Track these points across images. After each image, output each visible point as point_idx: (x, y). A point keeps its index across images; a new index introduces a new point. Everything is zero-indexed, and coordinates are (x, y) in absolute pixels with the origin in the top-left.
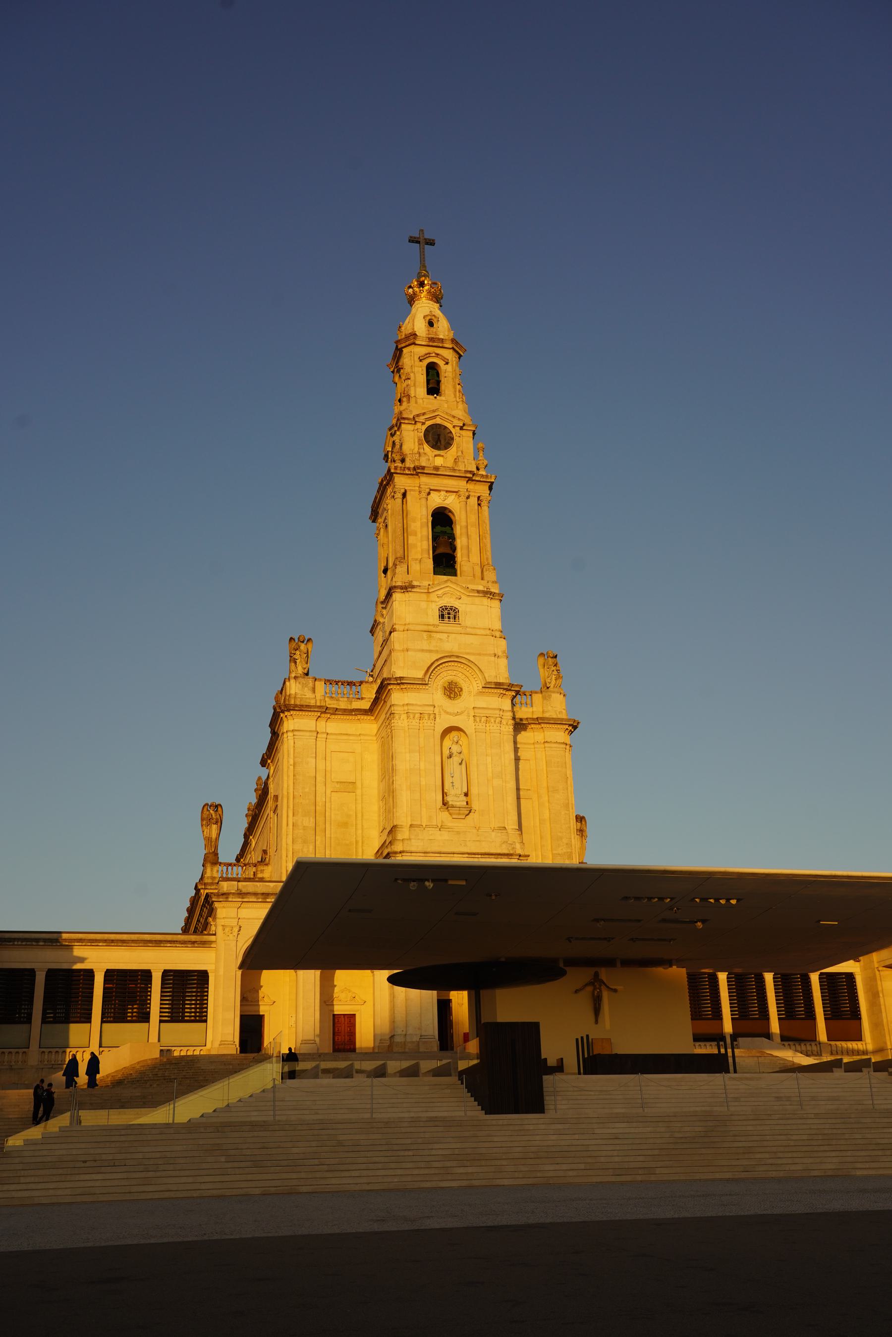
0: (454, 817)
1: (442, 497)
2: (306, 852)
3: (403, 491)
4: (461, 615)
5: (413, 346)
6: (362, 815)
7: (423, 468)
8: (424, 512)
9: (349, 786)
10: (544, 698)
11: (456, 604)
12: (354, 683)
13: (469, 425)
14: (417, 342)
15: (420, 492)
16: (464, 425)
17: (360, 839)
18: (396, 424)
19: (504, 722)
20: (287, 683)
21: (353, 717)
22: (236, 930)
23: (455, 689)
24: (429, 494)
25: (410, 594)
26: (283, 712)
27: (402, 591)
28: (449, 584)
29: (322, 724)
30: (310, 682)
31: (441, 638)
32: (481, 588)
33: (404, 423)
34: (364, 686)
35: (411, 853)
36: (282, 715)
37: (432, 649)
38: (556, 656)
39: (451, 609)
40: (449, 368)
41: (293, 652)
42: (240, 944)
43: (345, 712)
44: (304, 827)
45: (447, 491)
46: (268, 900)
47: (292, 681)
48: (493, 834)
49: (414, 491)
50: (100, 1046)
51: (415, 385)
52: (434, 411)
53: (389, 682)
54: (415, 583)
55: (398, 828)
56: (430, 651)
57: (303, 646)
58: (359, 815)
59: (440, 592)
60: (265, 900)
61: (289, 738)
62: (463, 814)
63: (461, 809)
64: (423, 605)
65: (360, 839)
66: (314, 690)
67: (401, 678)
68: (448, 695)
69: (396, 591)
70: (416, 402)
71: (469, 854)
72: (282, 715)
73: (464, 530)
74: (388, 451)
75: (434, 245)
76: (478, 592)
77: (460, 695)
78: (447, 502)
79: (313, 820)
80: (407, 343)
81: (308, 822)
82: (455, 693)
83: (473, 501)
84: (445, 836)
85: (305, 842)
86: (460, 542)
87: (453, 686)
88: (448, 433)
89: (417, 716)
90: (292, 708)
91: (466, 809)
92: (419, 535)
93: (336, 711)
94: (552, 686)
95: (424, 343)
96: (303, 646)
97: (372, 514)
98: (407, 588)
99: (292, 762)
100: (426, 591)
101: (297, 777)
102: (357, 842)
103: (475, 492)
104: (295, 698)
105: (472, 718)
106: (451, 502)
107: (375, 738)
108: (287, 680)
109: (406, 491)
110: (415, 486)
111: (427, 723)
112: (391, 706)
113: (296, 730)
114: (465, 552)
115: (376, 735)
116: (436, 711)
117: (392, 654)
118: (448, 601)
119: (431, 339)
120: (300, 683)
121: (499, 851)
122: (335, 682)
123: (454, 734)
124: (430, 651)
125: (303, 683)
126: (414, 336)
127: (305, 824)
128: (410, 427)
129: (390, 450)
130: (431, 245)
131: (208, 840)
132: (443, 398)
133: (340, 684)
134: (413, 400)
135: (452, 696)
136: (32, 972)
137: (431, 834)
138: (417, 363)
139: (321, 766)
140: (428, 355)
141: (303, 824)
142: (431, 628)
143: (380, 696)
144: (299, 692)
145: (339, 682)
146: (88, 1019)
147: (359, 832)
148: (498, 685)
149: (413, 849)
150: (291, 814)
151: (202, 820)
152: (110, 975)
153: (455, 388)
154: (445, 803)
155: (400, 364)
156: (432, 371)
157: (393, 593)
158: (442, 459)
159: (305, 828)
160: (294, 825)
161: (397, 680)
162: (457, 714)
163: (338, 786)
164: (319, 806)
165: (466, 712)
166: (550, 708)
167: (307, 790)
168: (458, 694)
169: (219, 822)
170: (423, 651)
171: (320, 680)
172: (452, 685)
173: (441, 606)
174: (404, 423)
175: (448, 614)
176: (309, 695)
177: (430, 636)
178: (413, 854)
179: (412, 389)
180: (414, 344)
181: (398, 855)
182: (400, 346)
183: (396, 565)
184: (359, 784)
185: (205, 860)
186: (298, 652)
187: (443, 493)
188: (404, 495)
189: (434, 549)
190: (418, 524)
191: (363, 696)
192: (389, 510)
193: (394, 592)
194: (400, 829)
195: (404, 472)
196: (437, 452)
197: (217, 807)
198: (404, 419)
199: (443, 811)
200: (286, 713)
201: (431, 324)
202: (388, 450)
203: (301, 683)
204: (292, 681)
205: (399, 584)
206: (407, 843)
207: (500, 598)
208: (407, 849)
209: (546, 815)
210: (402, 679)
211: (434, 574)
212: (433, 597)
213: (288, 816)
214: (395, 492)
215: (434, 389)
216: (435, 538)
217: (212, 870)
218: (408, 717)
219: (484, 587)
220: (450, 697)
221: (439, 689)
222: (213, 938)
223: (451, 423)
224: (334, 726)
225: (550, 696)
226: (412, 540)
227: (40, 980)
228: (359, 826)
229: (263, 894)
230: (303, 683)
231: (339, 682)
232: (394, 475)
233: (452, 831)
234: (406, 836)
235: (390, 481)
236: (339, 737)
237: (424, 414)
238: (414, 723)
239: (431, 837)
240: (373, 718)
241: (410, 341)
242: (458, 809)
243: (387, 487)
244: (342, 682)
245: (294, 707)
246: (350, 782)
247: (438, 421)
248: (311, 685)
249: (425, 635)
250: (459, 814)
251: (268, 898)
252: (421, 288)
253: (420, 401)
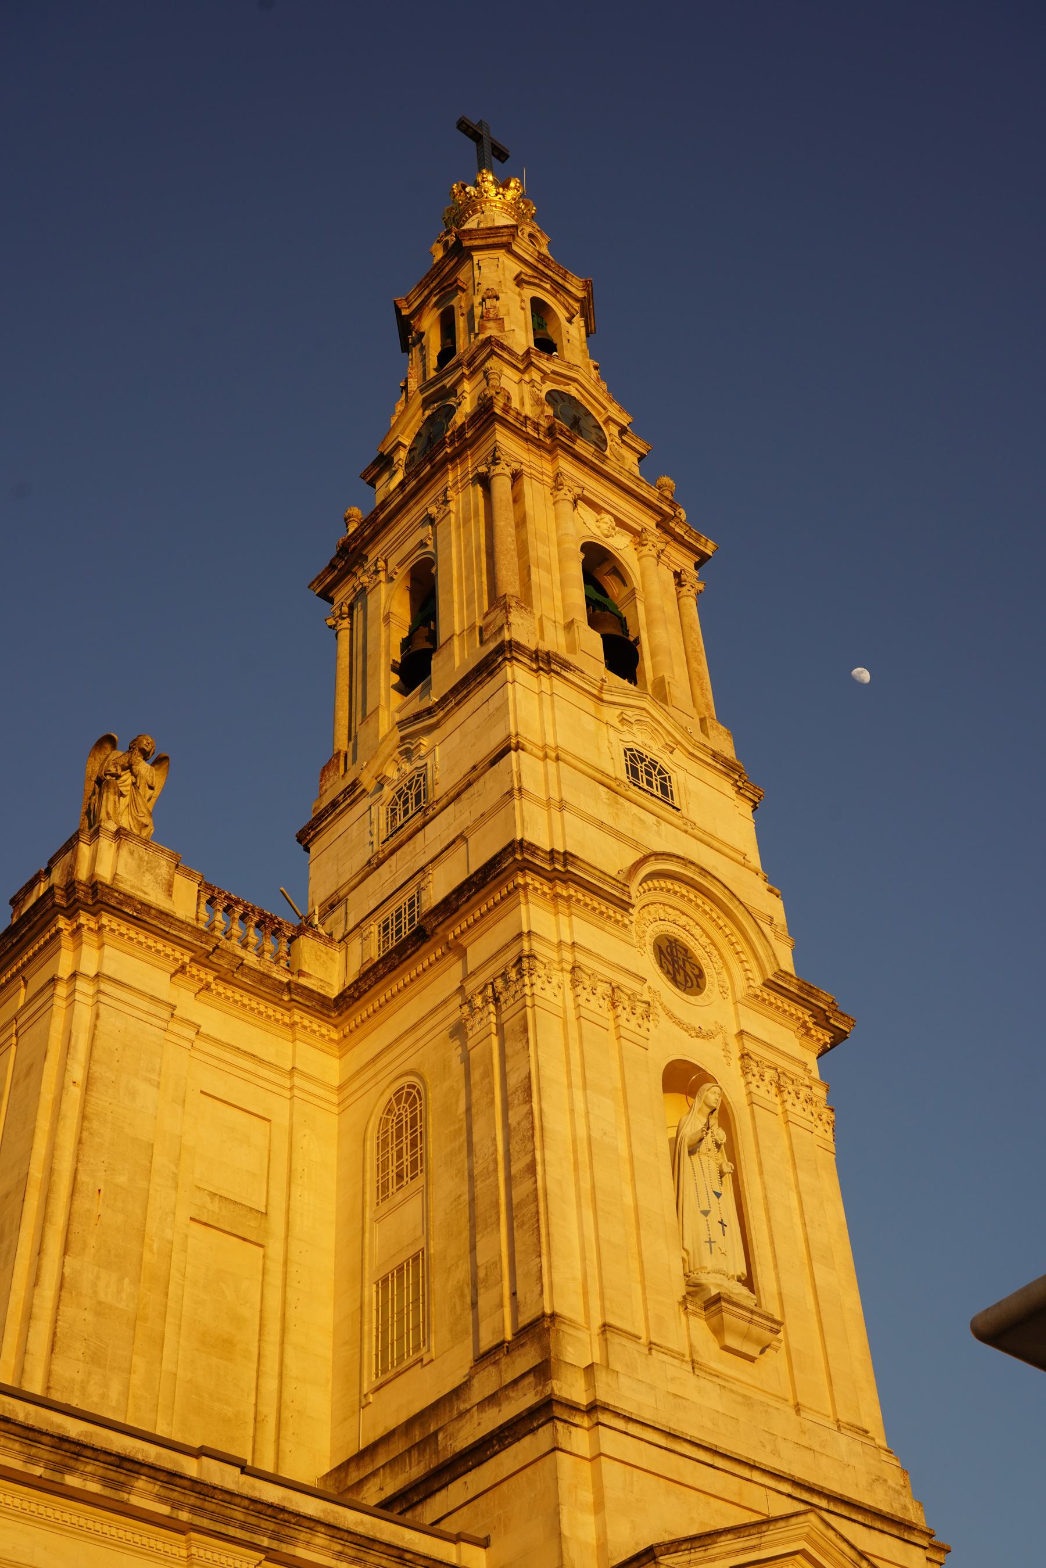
0: (731, 1341)
1: (604, 526)
2: (95, 1399)
5: (503, 251)
6: (284, 1330)
11: (665, 760)
12: (280, 923)
14: (515, 248)
17: (269, 1411)
18: (473, 358)
20: (85, 850)
21: (279, 1013)
23: (684, 964)
25: (557, 682)
26: (71, 914)
27: (534, 666)
31: (643, 817)
33: (500, 357)
34: (306, 944)
35: (629, 1419)
36: (62, 923)
39: (655, 768)
41: (113, 770)
43: (261, 982)
44: (100, 1303)
45: (620, 523)
46: (72, 1481)
47: (106, 844)
49: (542, 482)
53: (530, 858)
55: (565, 1323)
56: (618, 835)
58: (273, 1328)
60: (56, 1477)
61: (77, 996)
62: (758, 1341)
63: (755, 1317)
65: (269, 1411)
68: (668, 972)
69: (520, 658)
71: (796, 1484)
72: (62, 923)
74: (400, 444)
75: (503, 162)
77: (698, 986)
80: (490, 241)
82: (686, 974)
87: (680, 956)
88: (594, 427)
90: (113, 902)
91: (769, 1324)
96: (143, 767)
97: (332, 566)
99: (77, 1073)
100: (595, 692)
101: (95, 1125)
103: (668, 558)
105: (736, 1064)
106: (620, 544)
107: (335, 1099)
108: (85, 837)
110: (542, 473)
112: (520, 935)
113: (110, 979)
115: (340, 1088)
117: (516, 802)
120: (132, 853)
122: (227, 897)
124: (618, 835)
125: (141, 858)
126: (511, 230)
127: (102, 1296)
129: (407, 442)
130: (498, 158)
133: (239, 910)
135: (680, 978)
137: (673, 1379)
141: (95, 1293)
143: (439, 930)
144: (125, 875)
145: (237, 903)
147: (270, 1385)
155: (463, 275)
157: (507, 663)
159: (101, 1310)
160: (66, 1285)
161: (552, 860)
162: (700, 1034)
163: (215, 1206)
164: (151, 1251)
165: (719, 1038)
167: (122, 1180)
168: (695, 983)
170: (601, 825)
172: (677, 950)
173: (630, 746)
174: (500, 357)
178: (633, 1429)
180: (507, 247)
181: (577, 1420)
182: (467, 243)
183: (510, 607)
187: (607, 518)
188: (516, 477)
191: (305, 969)
192: (452, 516)
193: (510, 660)
194: (571, 1331)
195: (524, 429)
199: (695, 1314)
200: (83, 918)
202: (400, 439)
203: (136, 855)
206: (608, 1385)
207: (756, 800)
210: (573, 864)
213: (40, 1252)
214: (495, 461)
218: (575, 983)
220: (674, 981)
221: (647, 945)
223: (599, 413)
226: (537, 576)
230: (141, 858)
231: (237, 903)
232: (497, 426)
233: (732, 1391)
235: (470, 446)
236: (228, 1056)
238: (593, 1005)
239: (673, 1388)
240: (335, 1036)
241: (499, 239)
242: (749, 1315)
243: (450, 467)
244: (246, 907)
245: (121, 903)
246: (251, 1209)
247: (572, 390)
250: (746, 1337)
251: (72, 1470)
252: (501, 190)
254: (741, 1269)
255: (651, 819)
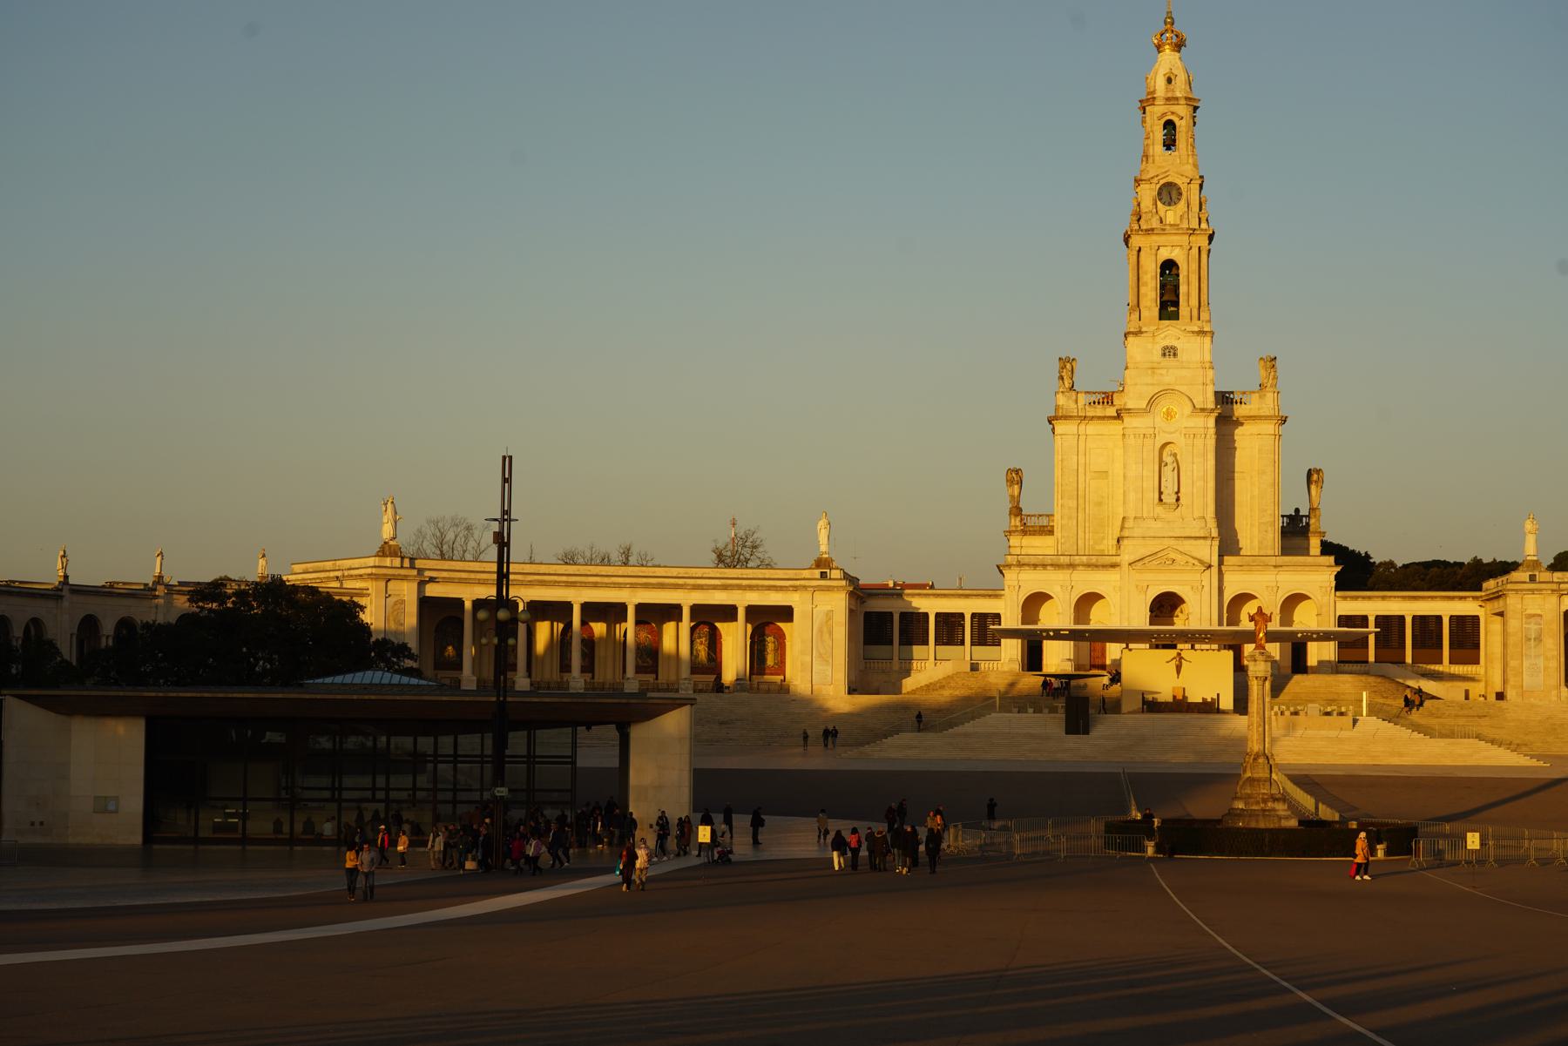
3: (1137, 249)
4: (1179, 352)
7: (1153, 230)
8: (1154, 266)
9: (1103, 474)
10: (1260, 397)
13: (1196, 179)
15: (1151, 249)
16: (1191, 180)
19: (1208, 436)
22: (1017, 588)
24: (1159, 249)
28: (1170, 328)
29: (1082, 427)
30: (1074, 393)
32: (1196, 329)
37: (1155, 382)
38: (1275, 358)
40: (1183, 122)
42: (1020, 597)
48: (1195, 522)
50: (935, 659)
51: (1153, 144)
52: (1166, 172)
54: (1144, 329)
56: (1153, 384)
57: (1068, 366)
58: (1110, 498)
59: (1162, 336)
64: (1150, 346)
66: (1076, 402)
67: (1129, 409)
70: (1154, 162)
73: (1185, 279)
76: (1193, 332)
78: (1173, 254)
79: (1075, 502)
81: (1073, 504)
83: (1195, 251)
84: (1159, 524)
85: (1070, 518)
86: (1183, 289)
89: (1142, 436)
92: (1149, 287)
93: (1092, 418)
94: (1269, 385)
95: (1161, 103)
98: (1139, 333)
99: (1060, 457)
102: (1108, 517)
104: (1062, 408)
106: (1176, 255)
109: (1140, 248)
111: (1148, 442)
114: (1186, 298)
116: (1156, 432)
118: (1168, 343)
119: (1168, 99)
121: (1198, 535)
123: (1168, 448)
124: (1153, 384)
128: (1147, 186)
131: (1012, 496)
132: (1176, 153)
134: (1150, 160)
136: (891, 614)
138: (1156, 122)
139: (1082, 461)
140: (1164, 114)
142: (1155, 365)
146: (926, 643)
148: (1203, 410)
149: (1135, 535)
150: (1060, 497)
151: (1007, 481)
152: (938, 615)
153: (1187, 142)
154: (1161, 500)
156: (1170, 125)
158: (1171, 215)
159: (1069, 508)
166: (1264, 405)
167: (1071, 480)
169: (1020, 483)
170: (1147, 384)
171: (1081, 392)
175: (1170, 352)
176: (1073, 405)
177: (1154, 372)
179: (1151, 147)
184: (1110, 472)
185: (1010, 514)
186: (1065, 370)
189: (1162, 295)
190: (1149, 276)
196: (1168, 208)
197: (1017, 471)
198: (1142, 180)
201: (1169, 81)
204: (1061, 394)
205: (1132, 330)
208: (1131, 535)
209: (1256, 492)
211: (1161, 318)
212: (1158, 339)
215: (1170, 144)
216: (1163, 286)
217: (1015, 520)
219: (1199, 327)
222: (1002, 592)
224: (1092, 428)
225: (1265, 395)
226: (1143, 290)
227: (896, 618)
228: (1110, 505)
229: (1033, 565)
234: (1131, 526)
237: (1157, 176)
247: (1169, 179)
248: (1074, 398)
249: (1150, 372)
253: (1157, 158)
254: (1176, 490)
255: (1164, 372)
